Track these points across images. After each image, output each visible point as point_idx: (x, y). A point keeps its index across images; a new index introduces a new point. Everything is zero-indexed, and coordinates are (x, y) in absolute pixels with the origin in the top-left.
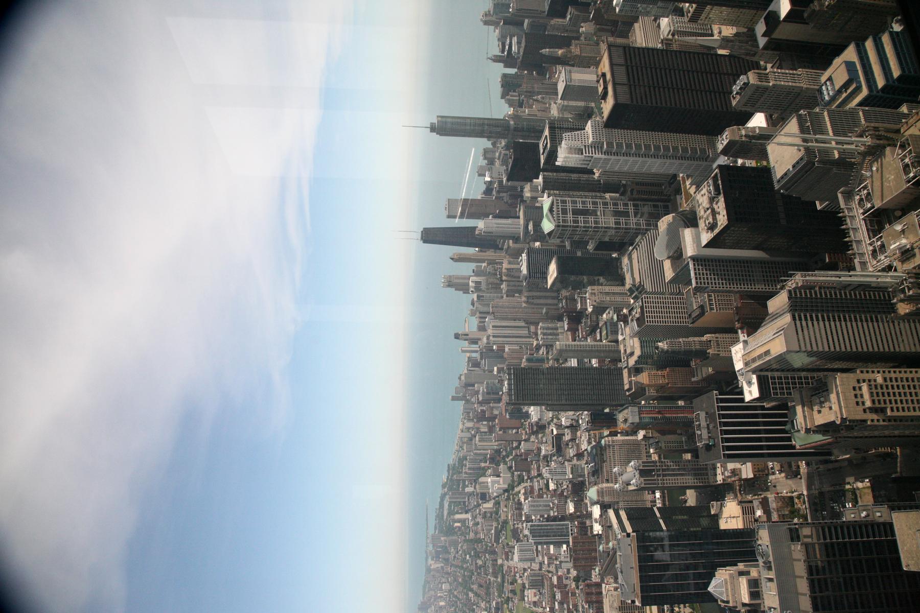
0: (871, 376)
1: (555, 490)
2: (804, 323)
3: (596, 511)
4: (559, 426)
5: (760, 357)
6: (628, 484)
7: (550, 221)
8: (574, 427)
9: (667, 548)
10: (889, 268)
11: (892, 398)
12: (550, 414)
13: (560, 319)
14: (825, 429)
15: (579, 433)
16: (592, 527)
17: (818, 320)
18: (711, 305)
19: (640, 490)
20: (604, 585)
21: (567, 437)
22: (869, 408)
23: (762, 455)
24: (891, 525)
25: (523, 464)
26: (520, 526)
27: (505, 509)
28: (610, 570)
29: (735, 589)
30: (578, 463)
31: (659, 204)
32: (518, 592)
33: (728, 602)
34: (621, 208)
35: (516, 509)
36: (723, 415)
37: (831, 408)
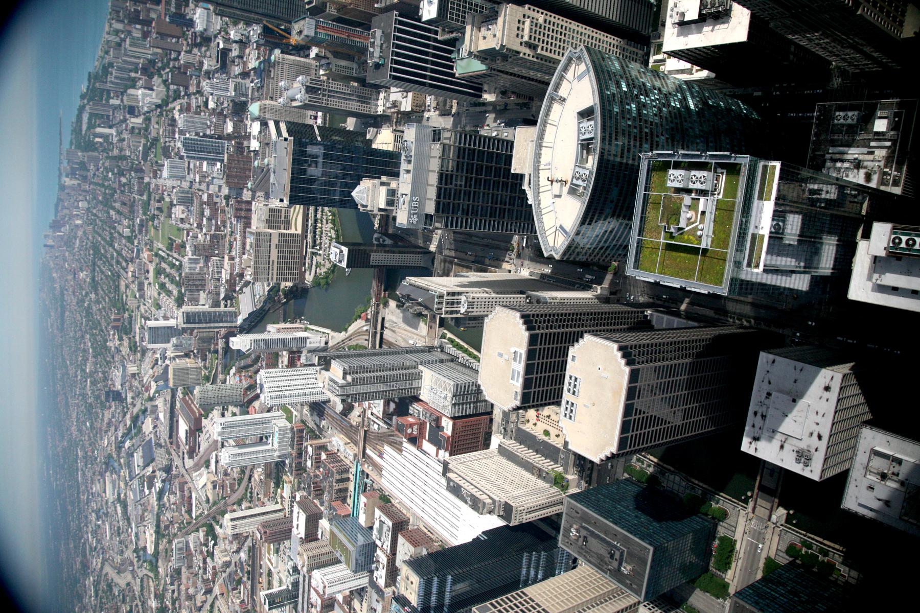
0: (535, 15)
1: (213, 109)
3: (255, 128)
4: (227, 40)
6: (293, 100)
8: (243, 43)
9: (320, 165)
11: (546, 39)
12: (217, 23)
14: (486, 56)
15: (247, 51)
19: (306, 107)
20: (254, 203)
21: (235, 53)
22: (526, 43)
23: (423, 84)
24: (512, 143)
25: (182, 76)
26: (172, 144)
27: (156, 126)
28: (264, 187)
29: (375, 196)
30: (243, 81)
32: (165, 210)
33: (366, 206)
35: (169, 125)
36: (400, 21)
37: (495, 36)
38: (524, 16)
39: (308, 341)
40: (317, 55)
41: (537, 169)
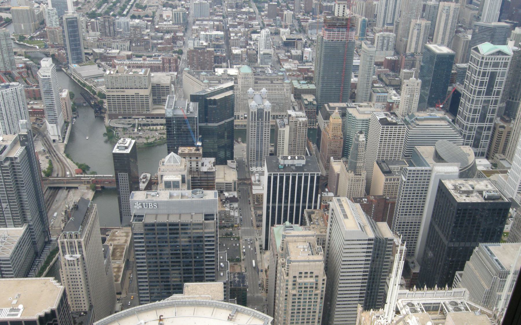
1: (251, 39)
2: (366, 246)
3: (233, 72)
5: (343, 211)
7: (490, 50)
8: (300, 58)
10: (398, 312)
13: (397, 53)
16: (221, 67)
17: (367, 256)
18: (391, 180)
19: (248, 110)
20: (176, 73)
21: (294, 52)
29: (172, 171)
31: (486, 149)
33: (163, 165)
34: (489, 116)
38: (317, 276)
39: (55, 125)
40: (290, 116)
41: (184, 304)
